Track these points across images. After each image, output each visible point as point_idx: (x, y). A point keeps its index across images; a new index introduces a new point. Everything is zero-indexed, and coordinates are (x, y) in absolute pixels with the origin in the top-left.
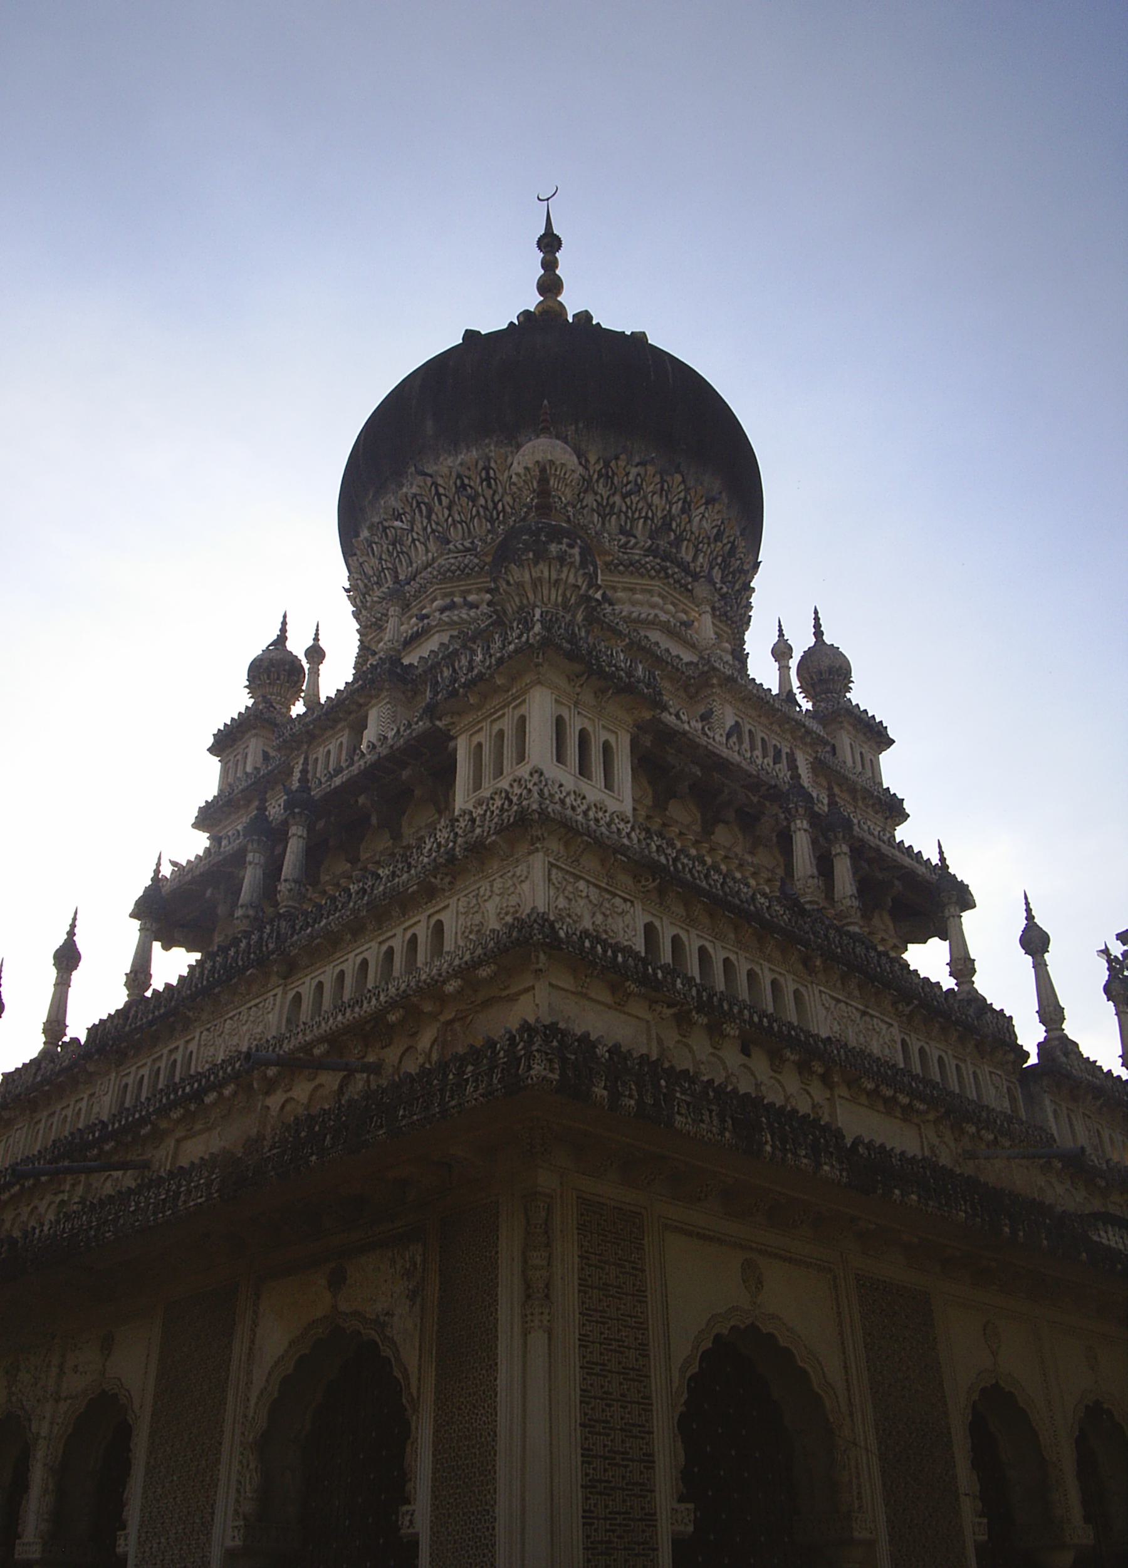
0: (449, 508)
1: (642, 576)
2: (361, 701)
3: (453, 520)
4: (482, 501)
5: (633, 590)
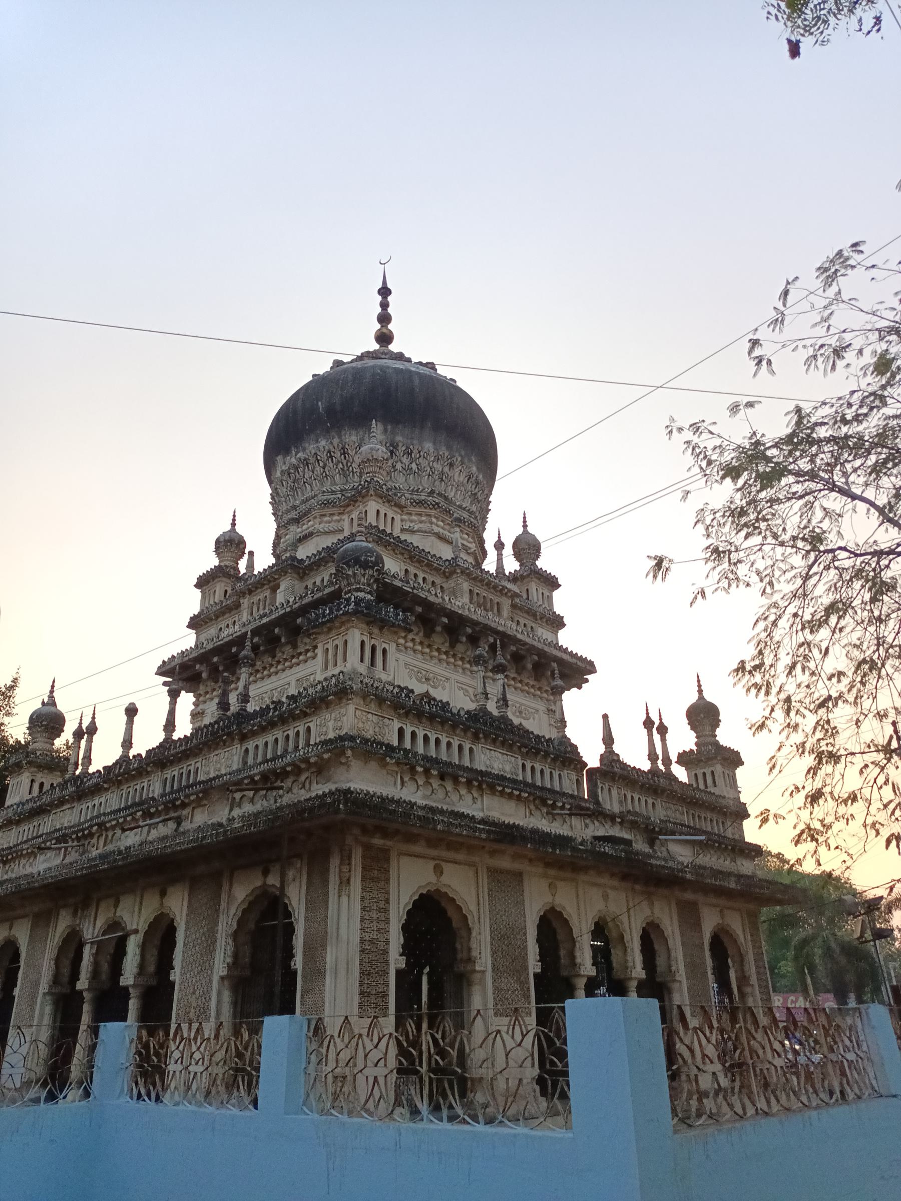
0: (324, 468)
2: (276, 577)
4: (340, 466)
5: (420, 515)
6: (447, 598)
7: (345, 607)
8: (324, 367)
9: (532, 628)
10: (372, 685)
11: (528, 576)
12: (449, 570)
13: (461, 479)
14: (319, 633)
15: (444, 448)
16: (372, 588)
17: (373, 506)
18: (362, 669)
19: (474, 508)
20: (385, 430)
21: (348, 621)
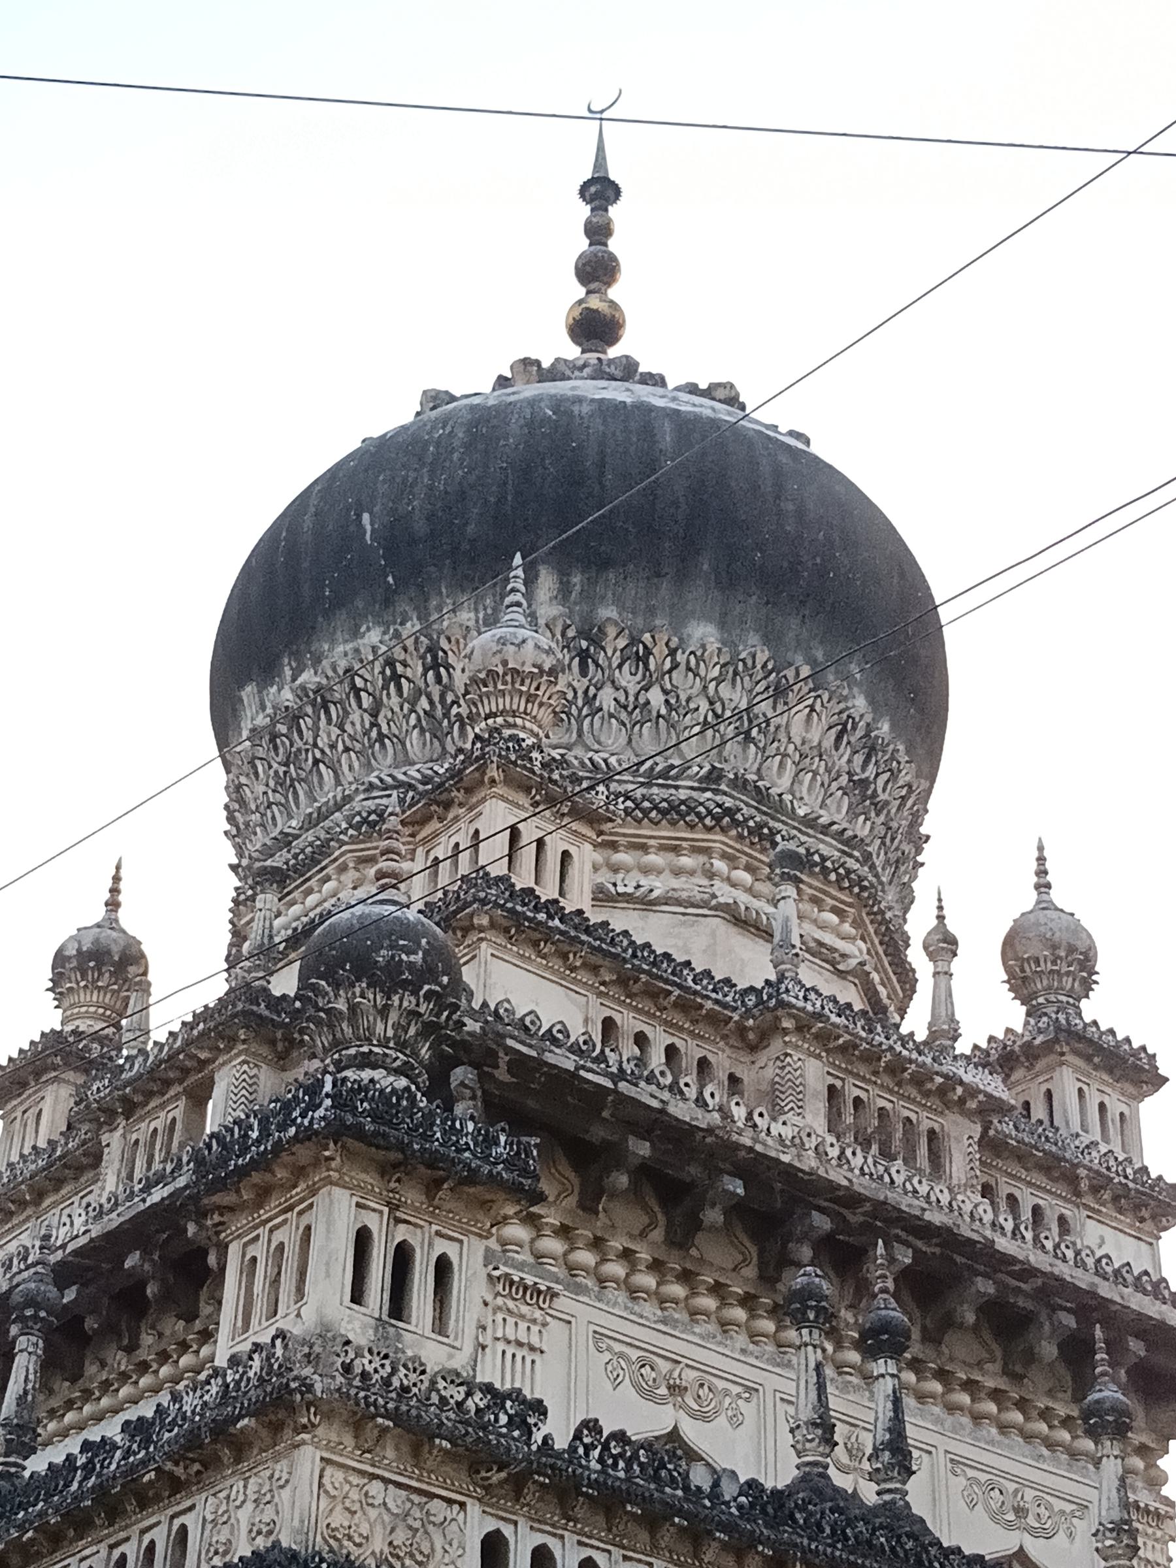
1: (691, 827)
3: (380, 733)
4: (424, 703)
5: (676, 850)
6: (739, 1113)
7: (303, 1115)
8: (396, 412)
9: (1062, 1220)
10: (387, 1382)
11: (1048, 1047)
12: (758, 1021)
13: (815, 736)
14: (231, 1209)
15: (754, 639)
16: (415, 1054)
17: (497, 813)
18: (357, 1325)
19: (861, 828)
20: (564, 592)
21: (317, 1163)
